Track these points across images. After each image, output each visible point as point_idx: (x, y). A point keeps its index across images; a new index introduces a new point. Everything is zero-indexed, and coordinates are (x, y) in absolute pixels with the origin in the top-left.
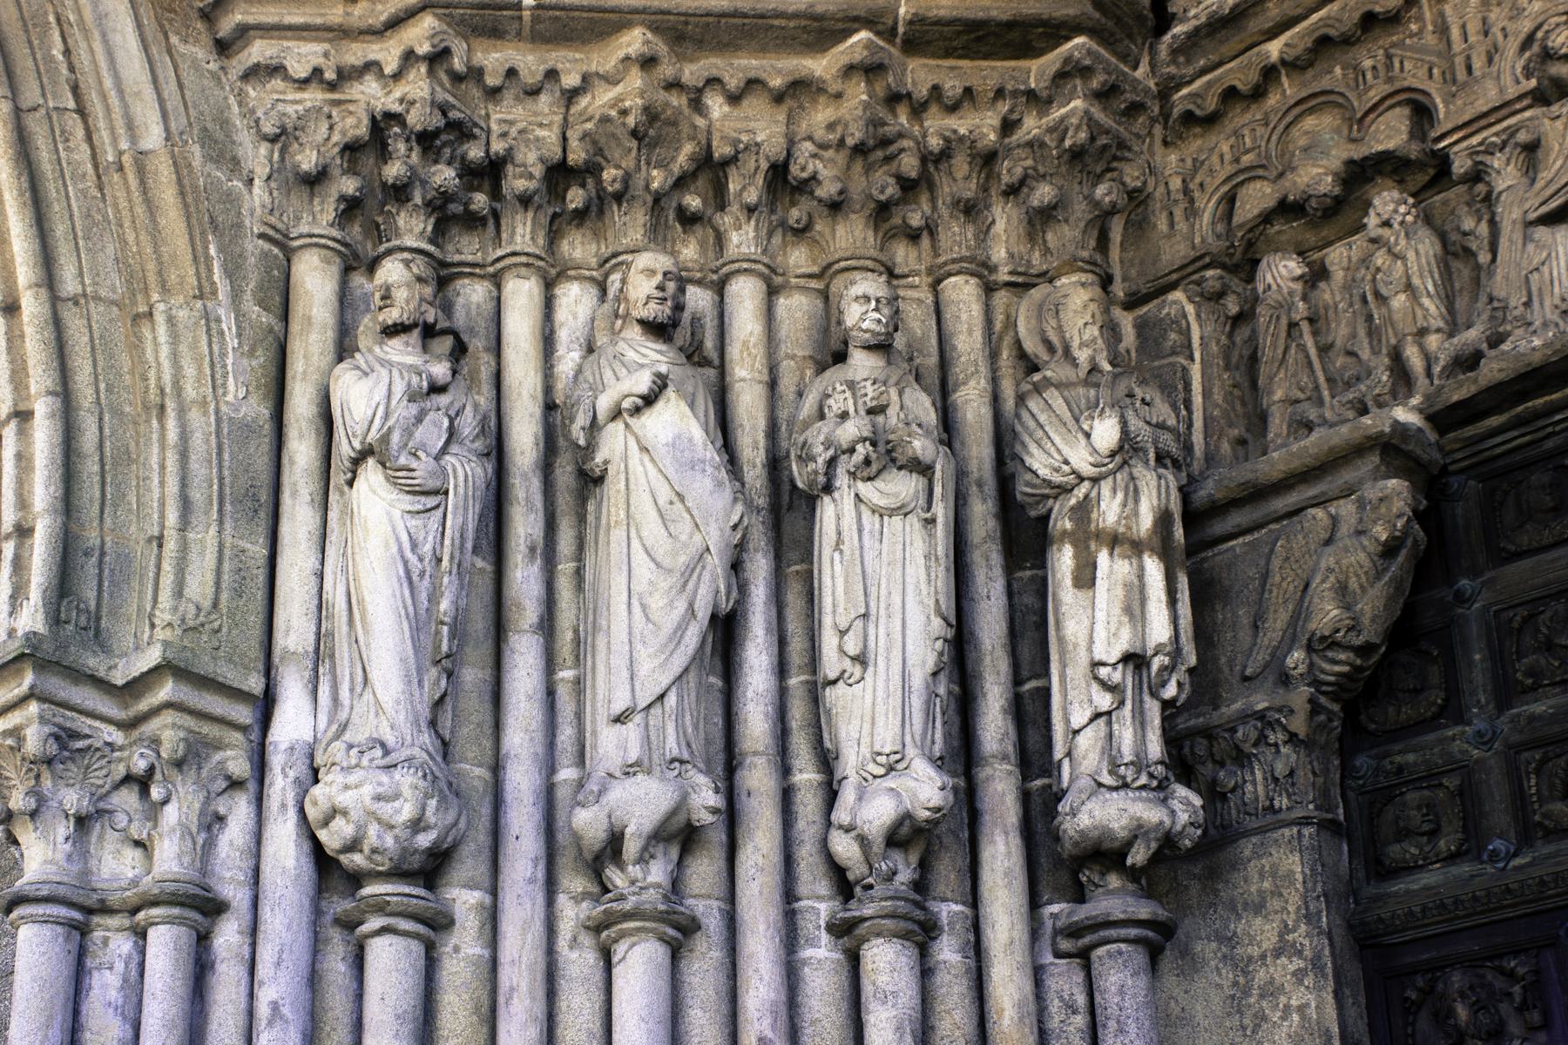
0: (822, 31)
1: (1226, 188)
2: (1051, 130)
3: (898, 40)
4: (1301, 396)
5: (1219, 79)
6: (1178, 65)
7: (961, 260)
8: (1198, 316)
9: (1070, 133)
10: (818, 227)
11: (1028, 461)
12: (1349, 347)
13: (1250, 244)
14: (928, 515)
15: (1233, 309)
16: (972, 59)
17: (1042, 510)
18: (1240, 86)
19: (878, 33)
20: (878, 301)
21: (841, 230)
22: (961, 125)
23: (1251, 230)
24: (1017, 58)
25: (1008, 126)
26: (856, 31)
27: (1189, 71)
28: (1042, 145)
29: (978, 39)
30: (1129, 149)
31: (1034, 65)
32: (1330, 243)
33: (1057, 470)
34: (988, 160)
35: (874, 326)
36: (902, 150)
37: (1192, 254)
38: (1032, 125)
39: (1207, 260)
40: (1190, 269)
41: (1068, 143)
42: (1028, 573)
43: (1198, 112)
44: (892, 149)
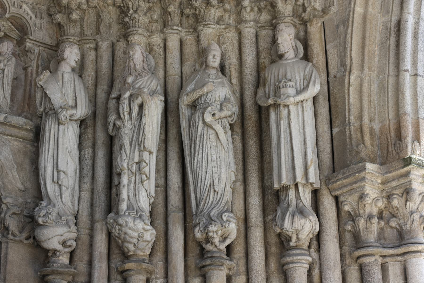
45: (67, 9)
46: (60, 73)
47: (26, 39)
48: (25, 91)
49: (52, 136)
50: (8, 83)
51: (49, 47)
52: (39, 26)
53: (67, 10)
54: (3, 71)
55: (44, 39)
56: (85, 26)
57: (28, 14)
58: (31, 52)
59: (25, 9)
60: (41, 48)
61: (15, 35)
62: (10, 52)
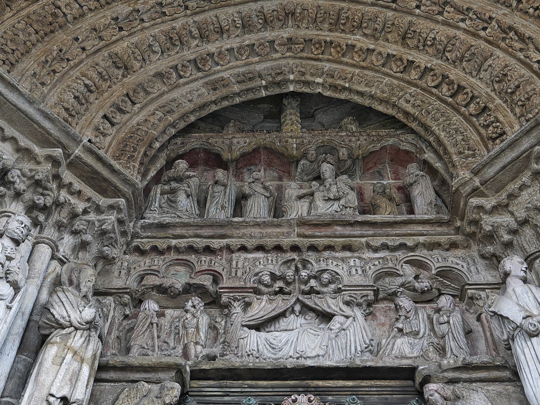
0: (47, 139)
1: (142, 273)
2: (99, 221)
3: (68, 161)
4: (146, 347)
5: (151, 242)
6: (141, 231)
7: (51, 240)
8: (115, 308)
9: (106, 224)
10: (6, 199)
11: (52, 310)
12: (166, 340)
13: (144, 294)
14: (10, 305)
15: (128, 312)
16: (86, 184)
17: (46, 332)
18: (159, 246)
19: (64, 153)
20: (25, 226)
21: (14, 204)
22: (73, 200)
23: (147, 289)
24: (99, 194)
25: (85, 212)
26: (58, 148)
27: (144, 235)
28: (93, 224)
29: (93, 178)
30: (117, 245)
31: (103, 199)
32: (168, 308)
33: (64, 318)
34: (74, 216)
35: (19, 233)
36: (49, 195)
37: (124, 286)
38: (92, 216)
39: (128, 290)
40: (120, 291)
41: (103, 227)
42: (24, 357)
43: (141, 247)
44: (46, 192)
45: (497, 239)
46: (509, 290)
47: (463, 286)
48: (486, 340)
49: (528, 356)
50: (459, 333)
51: (496, 286)
52: (476, 270)
53: (497, 240)
54: (448, 322)
55: (486, 279)
56: (525, 244)
57: (457, 264)
58: (478, 299)
59: (452, 261)
60: (487, 290)
61: (452, 291)
62: (451, 304)
